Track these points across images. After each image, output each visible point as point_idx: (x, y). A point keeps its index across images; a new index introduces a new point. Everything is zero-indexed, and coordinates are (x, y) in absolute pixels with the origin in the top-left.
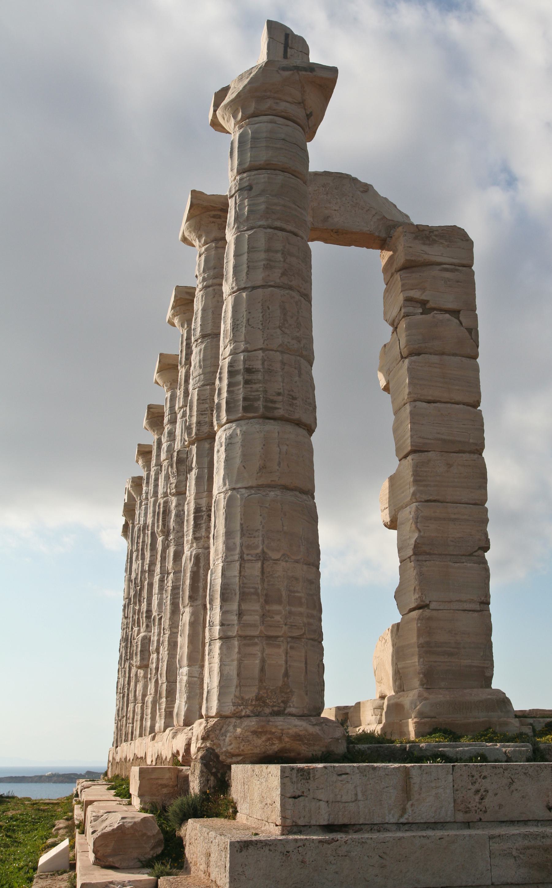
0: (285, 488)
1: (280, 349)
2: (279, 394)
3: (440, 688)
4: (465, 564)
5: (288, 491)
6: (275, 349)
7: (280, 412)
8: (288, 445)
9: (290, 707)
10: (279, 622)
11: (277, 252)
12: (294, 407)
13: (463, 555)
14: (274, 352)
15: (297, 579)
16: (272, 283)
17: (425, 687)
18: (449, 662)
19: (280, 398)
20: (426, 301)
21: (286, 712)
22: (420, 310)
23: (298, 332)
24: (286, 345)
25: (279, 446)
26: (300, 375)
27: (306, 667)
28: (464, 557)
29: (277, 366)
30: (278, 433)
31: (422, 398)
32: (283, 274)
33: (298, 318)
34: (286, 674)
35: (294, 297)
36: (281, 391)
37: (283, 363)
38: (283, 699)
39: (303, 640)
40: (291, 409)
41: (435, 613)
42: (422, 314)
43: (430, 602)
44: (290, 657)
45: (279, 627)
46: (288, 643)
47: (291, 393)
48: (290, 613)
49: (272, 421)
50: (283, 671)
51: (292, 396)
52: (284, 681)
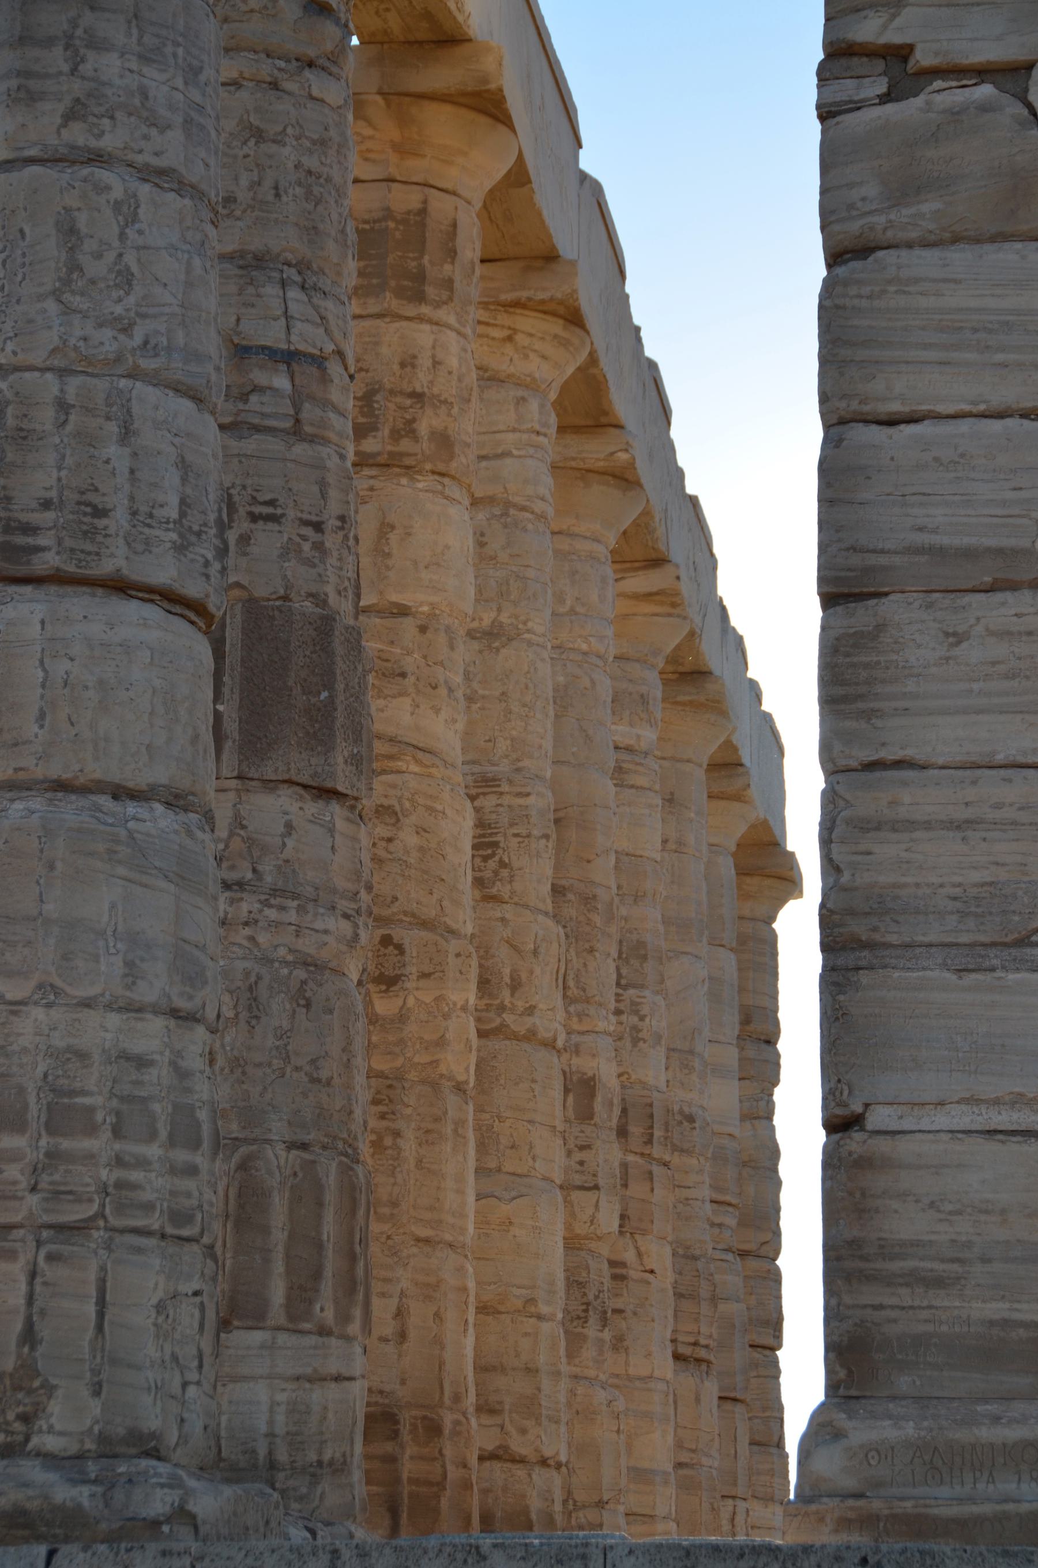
0: (61, 786)
1: (57, 362)
2: (46, 505)
3: (894, 1398)
4: (999, 974)
5: (73, 797)
6: (41, 365)
7: (50, 561)
8: (72, 660)
9: (40, 1431)
10: (15, 1183)
11: (49, 42)
12: (99, 538)
13: (994, 944)
14: (37, 374)
15: (83, 1056)
16: (33, 152)
17: (842, 1391)
18: (930, 1307)
19: (50, 515)
20: (901, 47)
21: (30, 1446)
22: (881, 86)
23: (120, 300)
24: (76, 348)
25: (42, 662)
26: (127, 434)
27: (101, 1315)
28: (992, 952)
29: (45, 417)
30: (43, 622)
31: (866, 408)
32: (69, 117)
33: (120, 255)
34: (29, 1336)
35: (108, 188)
36: (53, 494)
37: (63, 406)
38: (21, 1409)
39: (95, 1234)
40: (89, 547)
41: (883, 1145)
42: (885, 99)
43: (867, 1106)
44: (45, 1284)
45: (15, 1198)
46: (39, 1243)
47: (91, 497)
48: (53, 1155)
49: (28, 590)
50: (18, 1326)
51: (95, 507)
52: (19, 1356)
